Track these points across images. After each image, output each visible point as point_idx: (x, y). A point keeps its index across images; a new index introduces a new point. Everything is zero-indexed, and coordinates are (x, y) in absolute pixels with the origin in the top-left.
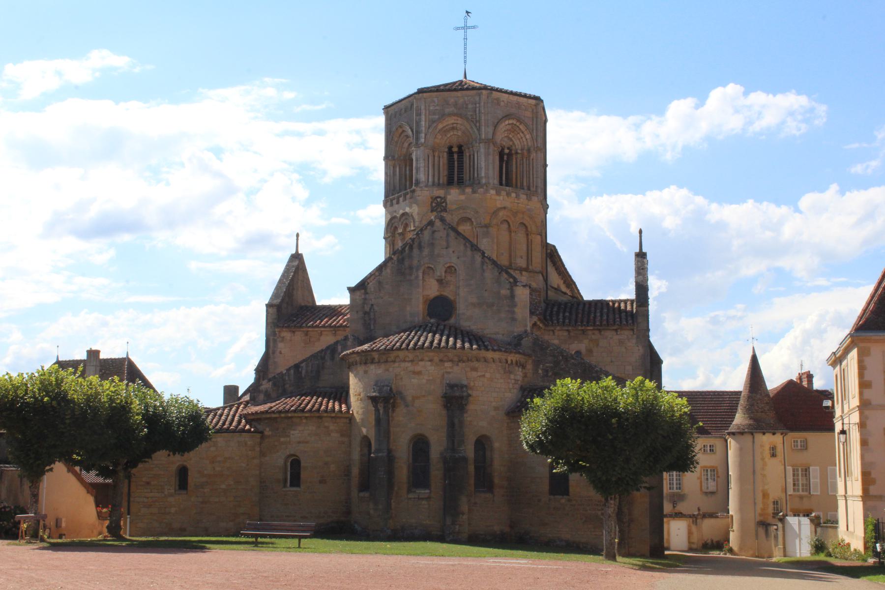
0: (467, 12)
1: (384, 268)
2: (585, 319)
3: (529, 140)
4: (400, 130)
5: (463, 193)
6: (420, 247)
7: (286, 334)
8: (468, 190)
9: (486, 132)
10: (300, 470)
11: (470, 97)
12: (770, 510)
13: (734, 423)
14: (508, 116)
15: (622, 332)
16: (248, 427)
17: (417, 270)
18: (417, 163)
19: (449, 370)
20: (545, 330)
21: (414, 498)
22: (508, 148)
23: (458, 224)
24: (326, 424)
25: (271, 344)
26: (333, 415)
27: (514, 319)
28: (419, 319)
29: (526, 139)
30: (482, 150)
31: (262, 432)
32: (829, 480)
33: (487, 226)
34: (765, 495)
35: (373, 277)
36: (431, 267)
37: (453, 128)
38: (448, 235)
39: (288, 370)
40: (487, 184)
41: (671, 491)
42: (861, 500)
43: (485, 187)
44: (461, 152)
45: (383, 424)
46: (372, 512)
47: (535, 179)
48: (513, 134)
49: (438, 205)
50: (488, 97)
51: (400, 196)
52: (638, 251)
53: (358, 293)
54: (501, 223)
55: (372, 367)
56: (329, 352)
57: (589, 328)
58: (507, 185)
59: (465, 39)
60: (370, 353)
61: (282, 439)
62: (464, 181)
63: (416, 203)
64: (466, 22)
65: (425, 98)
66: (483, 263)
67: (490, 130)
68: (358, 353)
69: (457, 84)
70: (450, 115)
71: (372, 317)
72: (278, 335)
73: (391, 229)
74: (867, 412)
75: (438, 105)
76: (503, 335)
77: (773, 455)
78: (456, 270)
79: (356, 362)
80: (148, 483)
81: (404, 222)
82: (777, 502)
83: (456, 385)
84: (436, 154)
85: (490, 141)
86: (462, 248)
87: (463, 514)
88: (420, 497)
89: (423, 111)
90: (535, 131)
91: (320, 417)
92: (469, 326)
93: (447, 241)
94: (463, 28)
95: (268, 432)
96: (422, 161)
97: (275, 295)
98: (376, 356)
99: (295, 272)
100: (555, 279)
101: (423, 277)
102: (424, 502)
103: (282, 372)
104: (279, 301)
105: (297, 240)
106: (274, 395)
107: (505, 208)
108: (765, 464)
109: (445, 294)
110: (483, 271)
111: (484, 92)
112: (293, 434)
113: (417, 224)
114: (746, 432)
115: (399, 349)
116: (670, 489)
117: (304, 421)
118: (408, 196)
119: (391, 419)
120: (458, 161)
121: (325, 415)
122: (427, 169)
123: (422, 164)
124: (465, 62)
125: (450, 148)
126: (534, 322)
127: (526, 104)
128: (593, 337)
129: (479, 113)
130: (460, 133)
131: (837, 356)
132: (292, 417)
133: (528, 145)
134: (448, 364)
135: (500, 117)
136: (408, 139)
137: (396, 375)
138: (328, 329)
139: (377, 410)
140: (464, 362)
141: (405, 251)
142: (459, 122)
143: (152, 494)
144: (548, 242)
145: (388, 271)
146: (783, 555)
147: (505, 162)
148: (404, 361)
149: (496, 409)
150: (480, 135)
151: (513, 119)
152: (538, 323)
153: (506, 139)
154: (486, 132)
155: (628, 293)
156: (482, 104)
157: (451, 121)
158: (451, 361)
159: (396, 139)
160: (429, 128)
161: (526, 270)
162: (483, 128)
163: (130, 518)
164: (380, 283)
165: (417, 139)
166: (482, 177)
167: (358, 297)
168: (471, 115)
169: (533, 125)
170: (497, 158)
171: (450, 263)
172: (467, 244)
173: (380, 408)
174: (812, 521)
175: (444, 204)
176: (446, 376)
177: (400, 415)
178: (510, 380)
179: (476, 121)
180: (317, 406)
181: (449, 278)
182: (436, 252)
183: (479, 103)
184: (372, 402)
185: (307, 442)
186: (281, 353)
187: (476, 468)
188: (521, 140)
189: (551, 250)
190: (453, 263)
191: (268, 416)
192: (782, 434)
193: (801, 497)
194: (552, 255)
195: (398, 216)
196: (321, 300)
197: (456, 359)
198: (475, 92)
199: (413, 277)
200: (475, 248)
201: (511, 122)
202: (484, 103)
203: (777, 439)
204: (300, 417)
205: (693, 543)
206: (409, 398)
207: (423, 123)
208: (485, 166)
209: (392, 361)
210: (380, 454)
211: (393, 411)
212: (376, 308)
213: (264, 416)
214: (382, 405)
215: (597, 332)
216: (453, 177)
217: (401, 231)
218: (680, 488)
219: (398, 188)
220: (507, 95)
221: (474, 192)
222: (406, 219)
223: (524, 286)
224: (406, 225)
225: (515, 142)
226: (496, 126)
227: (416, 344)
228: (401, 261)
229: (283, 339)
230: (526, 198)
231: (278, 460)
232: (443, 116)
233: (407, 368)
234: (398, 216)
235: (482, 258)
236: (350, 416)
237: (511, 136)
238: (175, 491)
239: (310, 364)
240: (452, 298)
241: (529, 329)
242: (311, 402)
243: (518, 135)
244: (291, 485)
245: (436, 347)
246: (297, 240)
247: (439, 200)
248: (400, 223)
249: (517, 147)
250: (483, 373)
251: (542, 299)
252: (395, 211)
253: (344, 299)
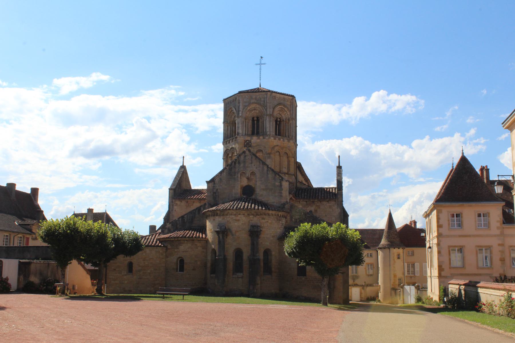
0: (261, 57)
1: (222, 173)
2: (314, 196)
3: (289, 115)
4: (231, 110)
5: (259, 139)
6: (239, 163)
7: (178, 202)
8: (261, 137)
9: (269, 111)
10: (184, 264)
11: (262, 96)
12: (397, 283)
13: (381, 243)
14: (279, 104)
15: (331, 202)
16: (160, 244)
17: (238, 174)
18: (238, 125)
19: (252, 219)
20: (296, 201)
21: (236, 277)
22: (279, 119)
23: (257, 152)
24: (196, 243)
25: (171, 207)
26: (199, 239)
27: (281, 196)
28: (238, 196)
29: (288, 115)
30: (268, 119)
31: (166, 247)
32: (424, 269)
33: (269, 154)
34: (395, 276)
35: (218, 176)
36: (244, 172)
37: (255, 109)
38: (252, 158)
39: (179, 218)
40: (270, 135)
41: (352, 274)
42: (437, 278)
43: (269, 136)
44: (258, 120)
45: (221, 243)
46: (216, 283)
47: (291, 133)
48: (282, 112)
49: (248, 144)
50: (270, 95)
51: (230, 140)
52: (338, 165)
53: (211, 184)
54: (276, 152)
55: (217, 217)
56: (197, 210)
57: (316, 200)
58: (279, 135)
59: (260, 69)
60: (215, 211)
61: (176, 250)
62: (259, 133)
63: (238, 143)
64: (261, 61)
65: (242, 96)
66: (267, 170)
67: (271, 110)
68: (210, 211)
69: (256, 89)
70: (253, 103)
71: (217, 195)
72: (174, 202)
73: (226, 155)
74: (440, 239)
75: (248, 99)
76: (276, 203)
77: (399, 258)
78: (255, 173)
79: (210, 215)
80: (115, 270)
81: (232, 152)
82: (400, 279)
83: (255, 226)
84: (247, 121)
85: (271, 115)
86: (258, 163)
87: (258, 284)
88: (239, 276)
89: (241, 102)
90: (291, 111)
91: (193, 240)
92: (261, 199)
93: (252, 160)
94: (259, 64)
95: (169, 247)
96: (240, 124)
97: (173, 185)
98: (218, 212)
99: (182, 174)
100: (300, 178)
101: (240, 177)
102: (240, 279)
103: (176, 220)
104: (175, 187)
105: (183, 159)
106: (172, 230)
107: (278, 145)
108: (395, 262)
109: (250, 184)
110: (268, 174)
111: (269, 93)
112: (181, 248)
113: (238, 152)
114: (386, 248)
115: (229, 209)
116: (352, 273)
117: (186, 242)
118: (234, 140)
119: (225, 241)
120: (256, 124)
121: (196, 239)
122: (242, 128)
123: (240, 125)
124: (260, 79)
125: (253, 118)
126: (290, 197)
127: (287, 99)
128: (318, 204)
129: (266, 102)
130: (257, 112)
131: (427, 213)
132: (180, 240)
133: (288, 117)
134: (251, 216)
135: (276, 104)
136: (234, 114)
137: (228, 221)
138: (197, 200)
139: (219, 237)
140: (259, 215)
141: (232, 165)
142: (257, 106)
144: (297, 161)
145: (224, 174)
146: (402, 303)
147: (278, 125)
148: (232, 215)
149: (273, 237)
150: (266, 112)
151: (282, 105)
152: (293, 198)
153: (278, 114)
154: (269, 111)
155: (333, 185)
156: (268, 99)
157: (253, 106)
158: (253, 215)
159: (228, 114)
160: (243, 109)
161: (287, 174)
162: (268, 109)
163: (106, 285)
164: (221, 179)
165: (238, 114)
166: (267, 132)
167: (210, 186)
168: (263, 103)
169: (291, 108)
170: (274, 123)
171: (253, 170)
172: (260, 162)
173: (220, 236)
174: (416, 287)
175: (250, 144)
176: (250, 221)
177: (229, 240)
178: (279, 224)
179: (265, 106)
180: (191, 235)
181: (252, 177)
182: (246, 165)
183: (266, 98)
184: (217, 233)
185: (187, 251)
187: (264, 264)
188: (285, 115)
189: (299, 165)
191: (169, 239)
192: (402, 248)
193: (411, 277)
194: (299, 167)
195: (229, 149)
196: (194, 187)
197: (255, 214)
198: (264, 93)
199: (236, 177)
200: (264, 163)
201: (281, 106)
202: (269, 98)
203: (400, 251)
204: (184, 240)
205: (362, 298)
206: (234, 232)
207: (241, 107)
208: (269, 126)
209: (225, 215)
210: (220, 257)
211: (226, 238)
212: (219, 190)
213: (167, 239)
214: (221, 235)
215: (319, 202)
216: (255, 131)
218: (356, 273)
219: (229, 136)
220: (279, 95)
221: (264, 138)
222: (233, 150)
223: (286, 181)
224: (233, 153)
225: (283, 116)
226: (274, 108)
227: (237, 207)
228: (230, 169)
229: (176, 205)
230: (287, 141)
231: (174, 259)
232: (250, 104)
233: (233, 218)
234: (229, 149)
235: (268, 168)
236: (207, 239)
237: (281, 113)
238: (127, 273)
239: (189, 216)
240: (253, 186)
241: (288, 200)
242: (189, 233)
243: (284, 113)
244: (180, 271)
245: (246, 209)
246: (183, 159)
247: (248, 142)
248: (230, 152)
249: (283, 118)
250: (267, 221)
251: (294, 187)
252: (228, 147)
253: (204, 187)
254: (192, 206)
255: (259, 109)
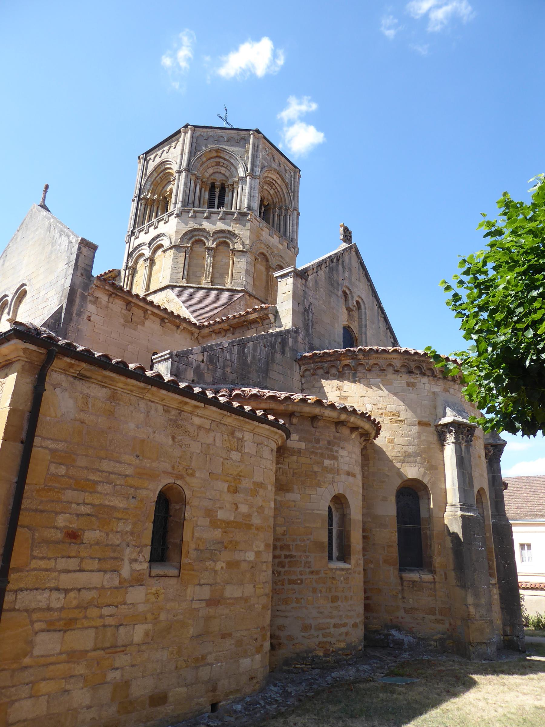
4: (214, 154)
25: (78, 300)
37: (271, 184)
55: (425, 380)
129: (294, 186)
142: (278, 181)
143: (82, 578)
157: (274, 176)
186: (90, 321)
190: (362, 299)
217: (214, 246)
222: (225, 237)
254: (139, 327)
255: (279, 190)
